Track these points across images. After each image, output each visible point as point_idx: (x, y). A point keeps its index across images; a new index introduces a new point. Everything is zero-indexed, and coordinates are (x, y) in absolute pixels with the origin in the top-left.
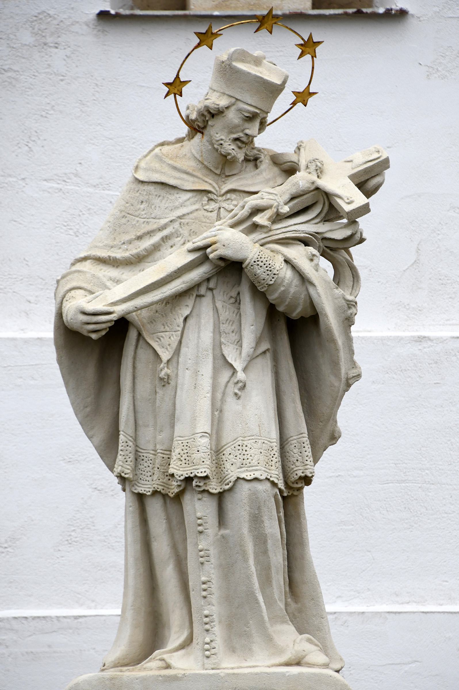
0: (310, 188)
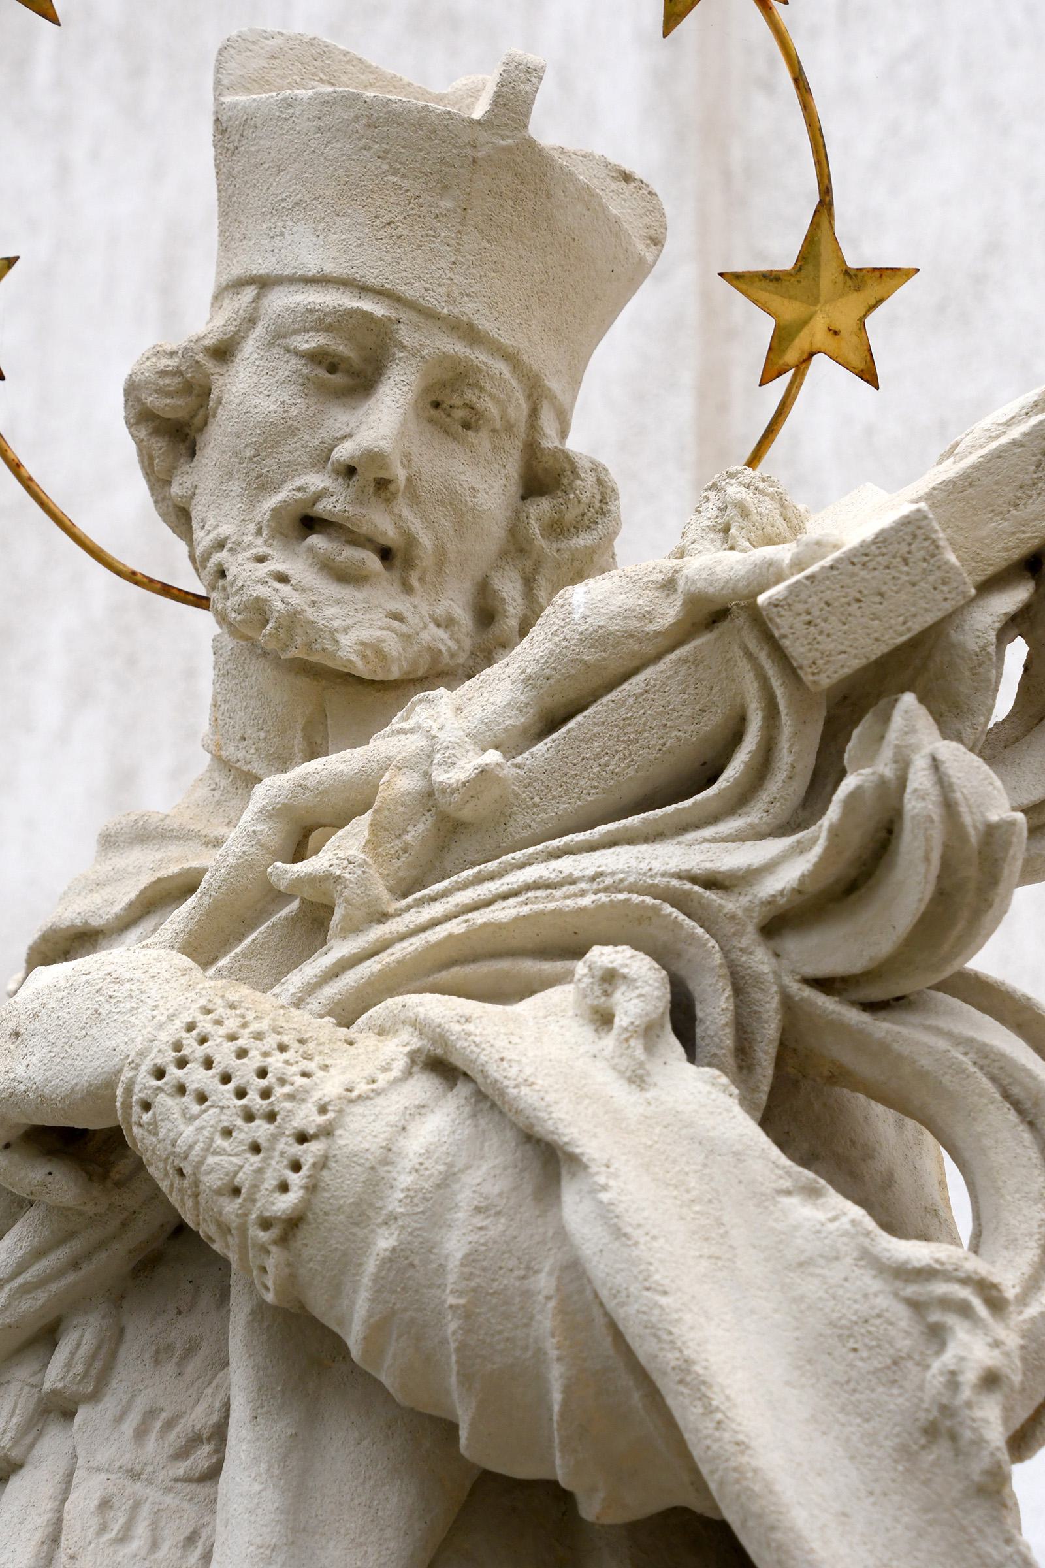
0: (648, 616)
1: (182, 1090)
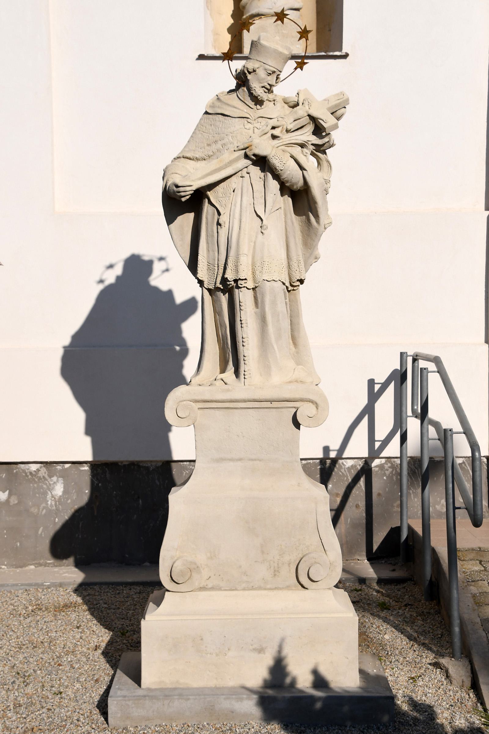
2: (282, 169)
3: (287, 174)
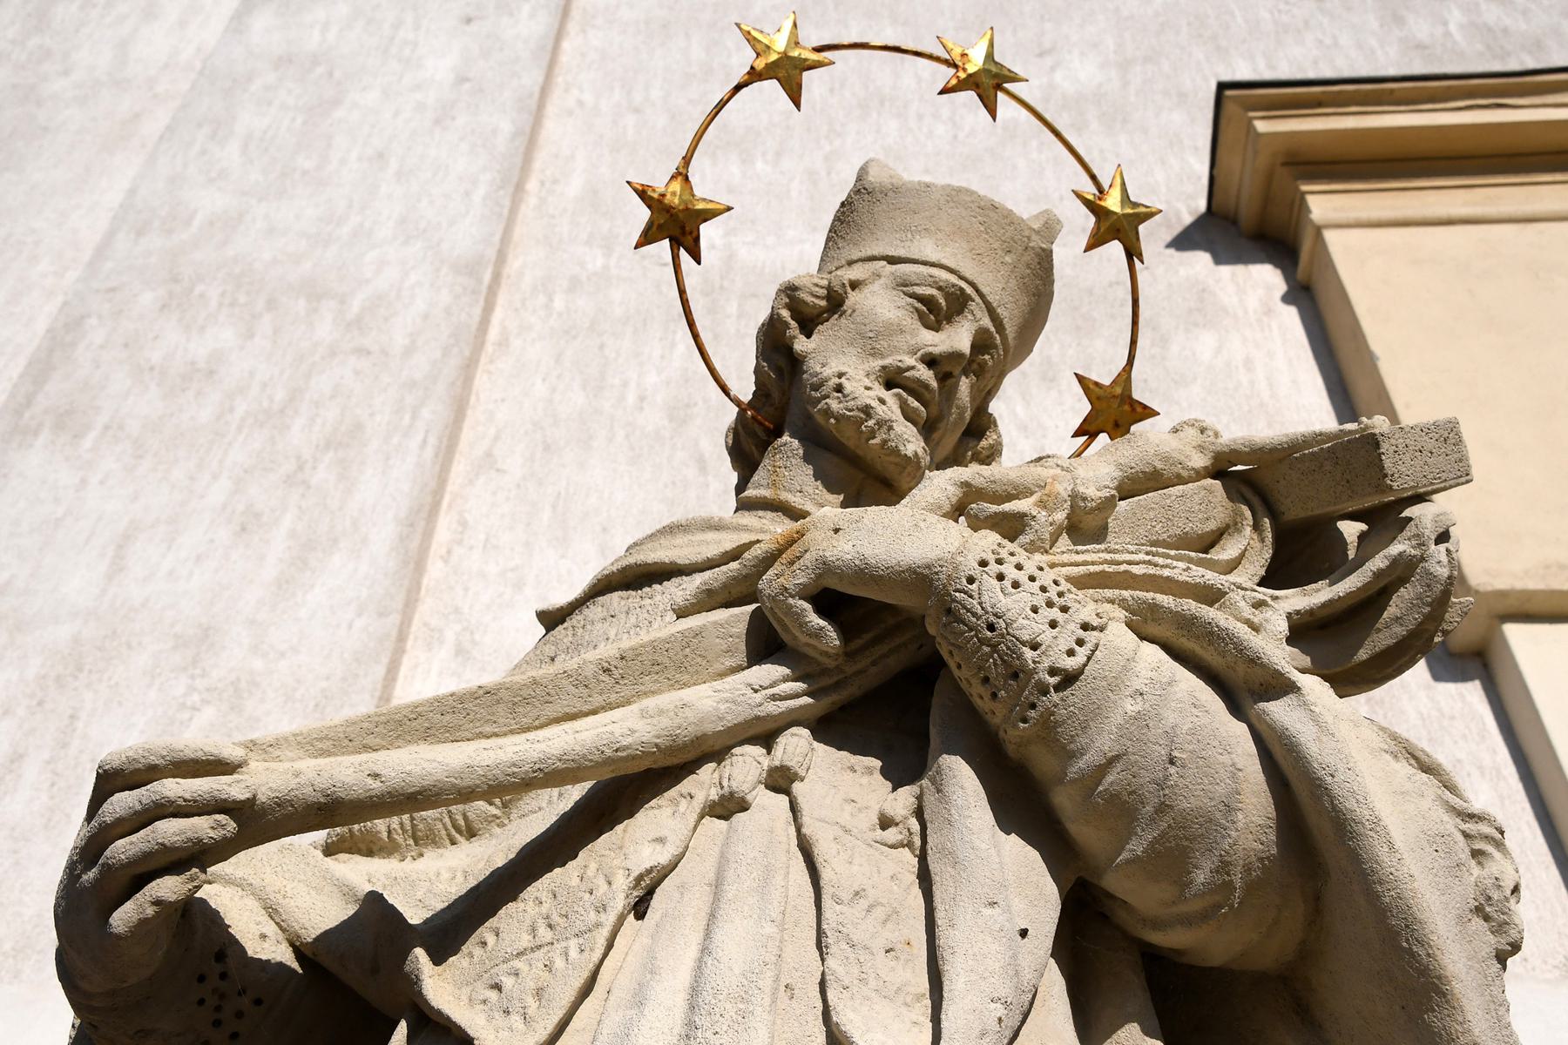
1: (1001, 577)
2: (1070, 663)
3: (1117, 718)
